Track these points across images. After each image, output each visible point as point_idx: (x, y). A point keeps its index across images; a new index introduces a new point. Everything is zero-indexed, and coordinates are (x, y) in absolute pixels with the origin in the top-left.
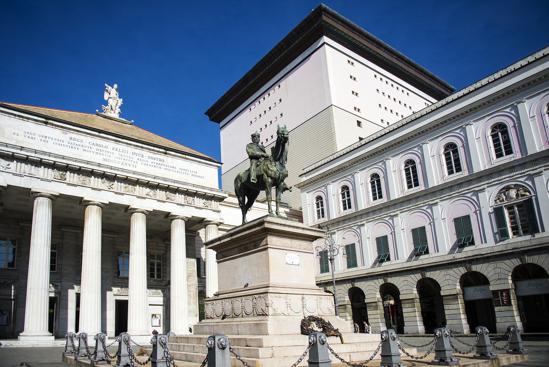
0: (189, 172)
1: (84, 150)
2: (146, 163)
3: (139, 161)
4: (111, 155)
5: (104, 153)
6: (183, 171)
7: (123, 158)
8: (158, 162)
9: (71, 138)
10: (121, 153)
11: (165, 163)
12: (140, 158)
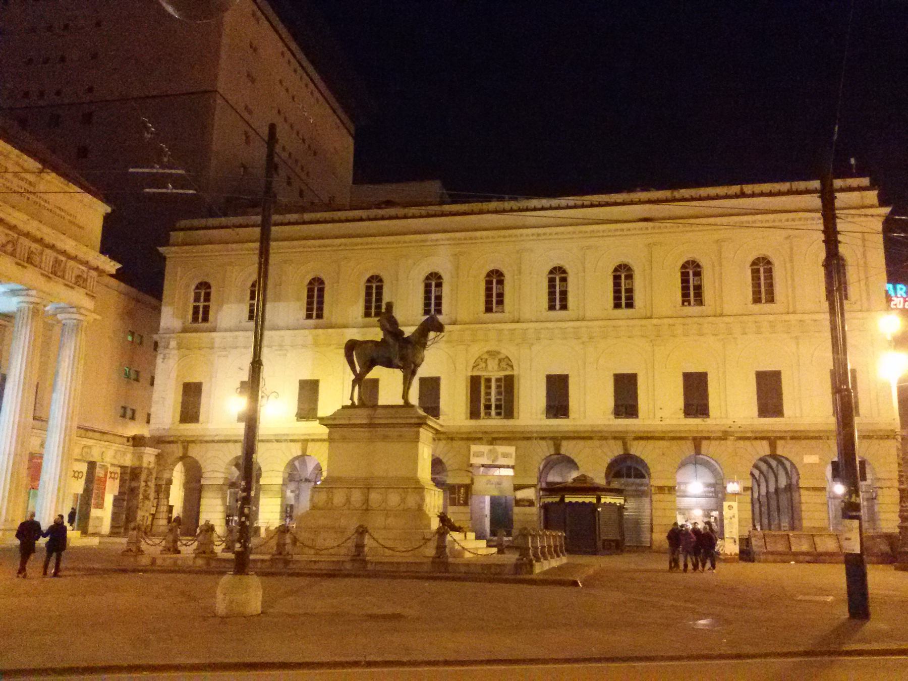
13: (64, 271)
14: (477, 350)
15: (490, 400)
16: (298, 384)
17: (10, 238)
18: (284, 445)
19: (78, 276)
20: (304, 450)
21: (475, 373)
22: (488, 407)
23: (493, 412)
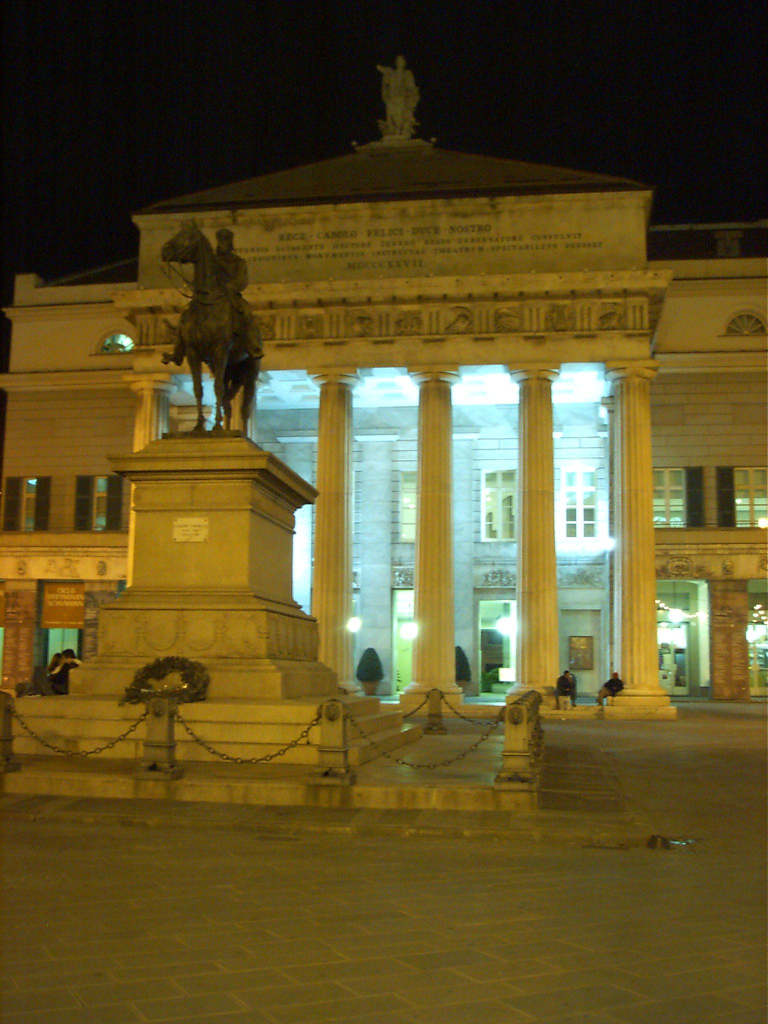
0: (559, 241)
1: (308, 256)
2: (444, 246)
3: (431, 247)
5: (350, 250)
6: (541, 242)
7: (392, 248)
8: (474, 235)
10: (387, 239)
11: (492, 233)
13: (572, 317)
17: (459, 312)
19: (604, 318)
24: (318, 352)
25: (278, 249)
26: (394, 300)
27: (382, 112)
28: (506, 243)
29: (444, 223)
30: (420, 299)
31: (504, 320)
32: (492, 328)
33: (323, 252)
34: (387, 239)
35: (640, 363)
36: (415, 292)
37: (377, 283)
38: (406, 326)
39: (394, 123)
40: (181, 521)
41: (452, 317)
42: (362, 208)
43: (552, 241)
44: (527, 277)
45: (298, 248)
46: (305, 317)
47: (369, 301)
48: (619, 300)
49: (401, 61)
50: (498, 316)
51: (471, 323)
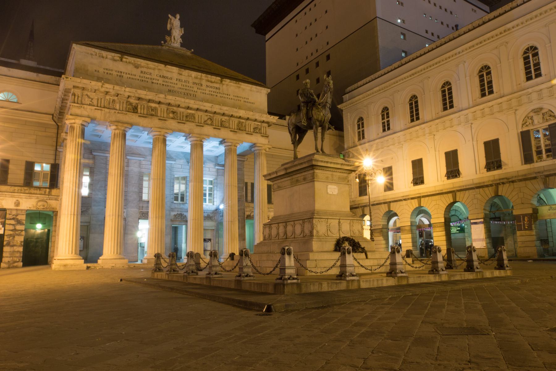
0: (241, 99)
1: (153, 83)
2: (204, 91)
3: (199, 91)
4: (175, 86)
5: (169, 84)
6: (236, 98)
7: (185, 88)
8: (215, 90)
9: (142, 72)
10: (183, 83)
11: (221, 91)
12: (200, 87)
13: (245, 127)
14: (523, 112)
15: (540, 147)
16: (411, 164)
17: (208, 117)
18: (409, 201)
19: (254, 129)
20: (420, 203)
21: (525, 129)
22: (539, 153)
23: (544, 155)
24: (156, 122)
25: (140, 76)
26: (188, 108)
27: (169, 33)
28: (225, 96)
29: (204, 83)
30: (198, 109)
31: (224, 123)
32: (220, 125)
33: (159, 82)
34: (183, 83)
35: (266, 146)
36: (196, 107)
37: (183, 100)
38: (189, 118)
39: (174, 39)
40: (329, 186)
41: (206, 118)
42: (175, 69)
43: (240, 99)
44: (235, 110)
45: (148, 78)
46: (151, 107)
47: (179, 106)
48: (259, 124)
49: (178, 16)
50: (222, 122)
51: (213, 122)
